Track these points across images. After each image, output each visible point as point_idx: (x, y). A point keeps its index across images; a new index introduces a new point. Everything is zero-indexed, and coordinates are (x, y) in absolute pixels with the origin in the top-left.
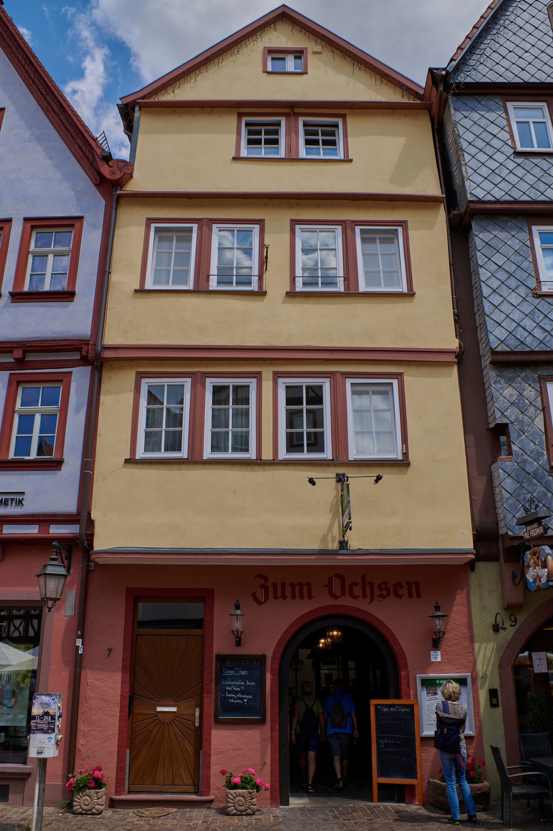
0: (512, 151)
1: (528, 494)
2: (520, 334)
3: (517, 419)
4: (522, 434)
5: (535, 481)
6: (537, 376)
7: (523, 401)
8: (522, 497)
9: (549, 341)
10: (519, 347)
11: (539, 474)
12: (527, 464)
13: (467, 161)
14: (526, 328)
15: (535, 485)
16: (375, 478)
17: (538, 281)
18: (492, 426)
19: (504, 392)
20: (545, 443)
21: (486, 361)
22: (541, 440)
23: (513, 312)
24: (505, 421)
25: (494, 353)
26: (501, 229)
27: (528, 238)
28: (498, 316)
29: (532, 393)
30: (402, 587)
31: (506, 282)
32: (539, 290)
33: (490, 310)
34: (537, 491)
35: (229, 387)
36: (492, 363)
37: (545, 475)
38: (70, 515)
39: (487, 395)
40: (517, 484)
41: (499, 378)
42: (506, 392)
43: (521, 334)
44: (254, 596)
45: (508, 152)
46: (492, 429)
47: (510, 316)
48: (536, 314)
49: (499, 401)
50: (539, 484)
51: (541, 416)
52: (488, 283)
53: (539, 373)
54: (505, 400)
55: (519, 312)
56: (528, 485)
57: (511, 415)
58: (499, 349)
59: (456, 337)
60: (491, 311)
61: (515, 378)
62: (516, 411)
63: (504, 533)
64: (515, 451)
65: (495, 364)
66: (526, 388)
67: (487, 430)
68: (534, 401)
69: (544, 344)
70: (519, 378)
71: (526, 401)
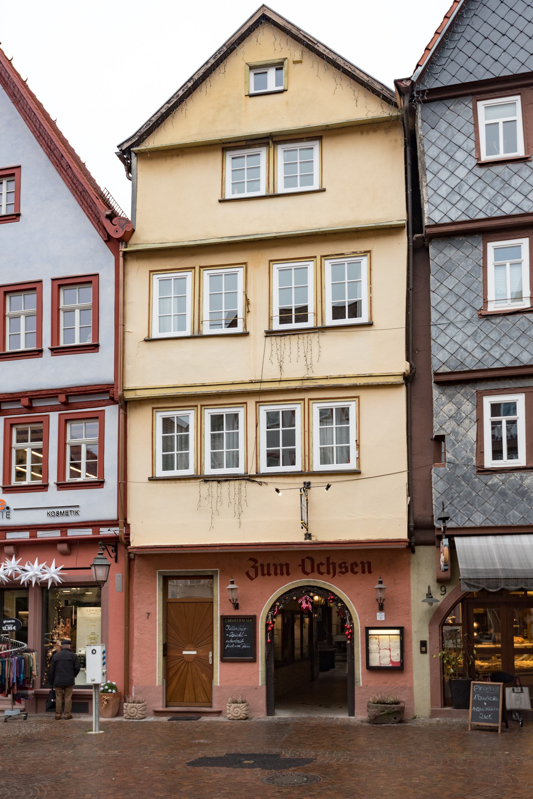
0: (474, 162)
1: (456, 493)
4: (456, 443)
5: (463, 483)
6: (475, 391)
7: (461, 414)
8: (450, 496)
10: (458, 367)
11: (467, 477)
12: (457, 469)
13: (428, 181)
14: (467, 349)
15: (463, 486)
16: (326, 487)
17: (485, 301)
19: (444, 408)
20: (475, 451)
22: (472, 447)
23: (457, 334)
24: (442, 433)
25: (436, 374)
26: (456, 250)
27: (482, 256)
28: (442, 340)
29: (468, 407)
31: (454, 305)
32: (485, 310)
33: (436, 335)
34: (464, 491)
35: (223, 415)
37: (471, 477)
38: (113, 521)
40: (447, 486)
43: (462, 355)
44: (247, 574)
45: (471, 164)
46: (434, 439)
47: (454, 339)
48: (479, 335)
49: (439, 416)
50: (466, 485)
52: (438, 308)
55: (462, 334)
56: (457, 486)
57: (448, 428)
58: (440, 371)
59: (408, 359)
60: (437, 336)
61: (456, 394)
62: (453, 423)
64: (449, 459)
65: (438, 383)
66: (464, 403)
67: (432, 439)
68: (470, 414)
69: (482, 363)
70: (459, 395)
71: (463, 415)
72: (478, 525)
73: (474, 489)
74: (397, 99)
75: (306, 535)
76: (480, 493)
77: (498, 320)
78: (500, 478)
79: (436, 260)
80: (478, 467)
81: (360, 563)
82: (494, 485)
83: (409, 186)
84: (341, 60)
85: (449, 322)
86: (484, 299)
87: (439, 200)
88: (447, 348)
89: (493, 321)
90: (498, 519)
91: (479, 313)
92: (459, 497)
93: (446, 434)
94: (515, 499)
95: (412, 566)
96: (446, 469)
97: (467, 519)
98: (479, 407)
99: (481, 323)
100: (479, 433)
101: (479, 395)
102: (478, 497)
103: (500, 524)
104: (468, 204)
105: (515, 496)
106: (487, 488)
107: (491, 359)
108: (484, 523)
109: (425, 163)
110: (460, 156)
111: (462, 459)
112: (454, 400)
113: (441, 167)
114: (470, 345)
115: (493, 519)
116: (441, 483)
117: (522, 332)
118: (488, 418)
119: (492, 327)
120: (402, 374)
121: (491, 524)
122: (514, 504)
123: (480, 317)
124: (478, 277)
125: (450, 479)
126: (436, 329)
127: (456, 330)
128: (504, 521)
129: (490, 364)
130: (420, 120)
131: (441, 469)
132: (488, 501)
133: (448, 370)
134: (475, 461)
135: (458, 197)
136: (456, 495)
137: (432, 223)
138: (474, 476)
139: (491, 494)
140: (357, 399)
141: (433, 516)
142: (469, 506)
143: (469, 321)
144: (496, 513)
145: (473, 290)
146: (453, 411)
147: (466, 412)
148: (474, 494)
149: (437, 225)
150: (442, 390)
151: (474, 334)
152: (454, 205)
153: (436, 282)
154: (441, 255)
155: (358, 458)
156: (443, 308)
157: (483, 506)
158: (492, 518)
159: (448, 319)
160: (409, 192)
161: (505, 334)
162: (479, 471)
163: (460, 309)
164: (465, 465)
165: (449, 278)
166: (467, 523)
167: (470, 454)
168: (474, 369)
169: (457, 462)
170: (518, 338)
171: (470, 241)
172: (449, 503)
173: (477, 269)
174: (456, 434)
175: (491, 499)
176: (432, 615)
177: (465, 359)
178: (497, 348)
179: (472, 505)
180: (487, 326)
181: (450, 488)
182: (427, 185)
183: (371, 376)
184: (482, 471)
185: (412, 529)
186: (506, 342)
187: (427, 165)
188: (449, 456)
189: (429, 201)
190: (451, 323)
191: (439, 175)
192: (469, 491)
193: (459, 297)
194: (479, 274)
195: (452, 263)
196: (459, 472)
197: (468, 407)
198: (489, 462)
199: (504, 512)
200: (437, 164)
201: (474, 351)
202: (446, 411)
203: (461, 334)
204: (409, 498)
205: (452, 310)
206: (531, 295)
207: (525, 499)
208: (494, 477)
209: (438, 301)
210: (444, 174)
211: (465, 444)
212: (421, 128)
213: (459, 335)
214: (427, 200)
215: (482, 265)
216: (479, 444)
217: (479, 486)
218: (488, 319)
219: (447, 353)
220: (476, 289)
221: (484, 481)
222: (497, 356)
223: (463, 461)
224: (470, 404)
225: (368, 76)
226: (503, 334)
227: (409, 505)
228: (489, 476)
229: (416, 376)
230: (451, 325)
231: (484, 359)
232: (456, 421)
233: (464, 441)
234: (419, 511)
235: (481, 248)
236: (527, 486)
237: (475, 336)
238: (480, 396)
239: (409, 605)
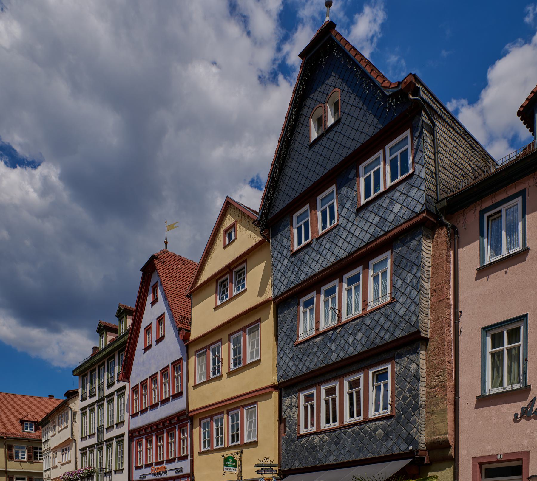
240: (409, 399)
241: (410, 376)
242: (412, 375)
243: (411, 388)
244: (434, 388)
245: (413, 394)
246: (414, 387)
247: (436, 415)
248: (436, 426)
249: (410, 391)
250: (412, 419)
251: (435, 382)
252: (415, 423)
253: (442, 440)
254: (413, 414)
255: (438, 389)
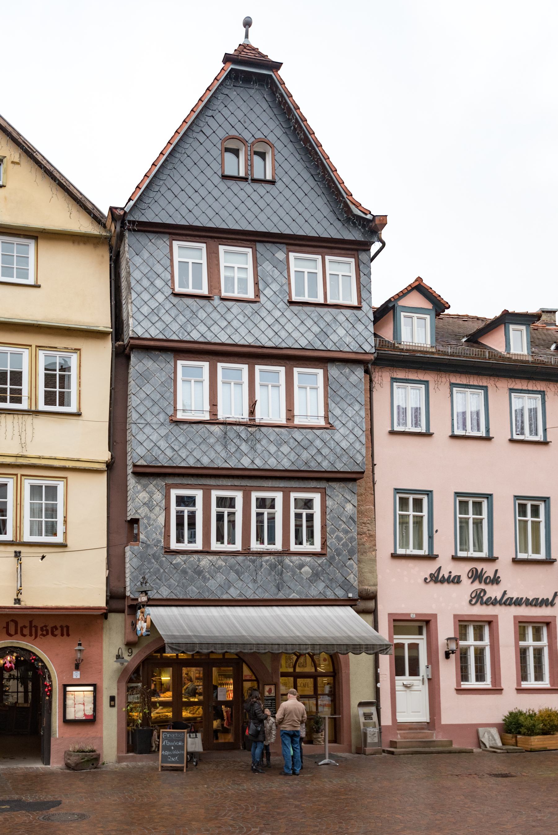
1: (147, 569)
2: (156, 451)
3: (146, 516)
4: (148, 526)
5: (153, 561)
6: (164, 484)
7: (152, 502)
8: (143, 571)
9: (176, 458)
12: (149, 548)
15: (153, 563)
18: (129, 519)
19: (140, 495)
21: (130, 470)
24: (137, 516)
25: (135, 466)
29: (159, 497)
30: (57, 629)
36: (134, 473)
37: (160, 557)
39: (128, 495)
41: (137, 484)
42: (140, 495)
46: (129, 521)
47: (150, 437)
50: (155, 563)
51: (164, 514)
53: (166, 482)
54: (139, 501)
56: (148, 563)
57: (142, 513)
58: (139, 463)
59: (109, 450)
61: (149, 485)
62: (146, 509)
63: (129, 595)
64: (142, 539)
65: (135, 473)
67: (126, 521)
68: (160, 503)
71: (155, 502)
72: (165, 597)
73: (161, 566)
74: (109, 222)
75: (15, 600)
76: (166, 571)
77: (185, 427)
78: (182, 558)
79: (136, 368)
80: (166, 548)
81: (60, 627)
82: (178, 564)
83: (113, 298)
84: (58, 173)
85: (146, 422)
86: (174, 408)
87: (142, 318)
88: (144, 444)
89: (181, 426)
90: (180, 593)
91: (171, 419)
92: (150, 573)
93: (140, 517)
94: (193, 576)
95: (105, 630)
96: (138, 548)
97: (156, 591)
98: (167, 498)
99: (172, 427)
100: (167, 520)
101: (167, 487)
102: (165, 574)
103: (181, 597)
104: (165, 326)
105: (194, 574)
106: (172, 566)
107: (179, 458)
108: (170, 595)
109: (130, 282)
110: (159, 283)
111: (153, 541)
112: (147, 489)
113: (143, 289)
114: (163, 444)
115: (176, 593)
116: (135, 560)
117: (203, 439)
118: (174, 508)
119: (180, 431)
120: (106, 462)
121: (175, 597)
122: (192, 580)
123: (171, 422)
124: (169, 388)
125: (143, 557)
126: (136, 427)
127: (152, 431)
128: (184, 595)
129: (178, 462)
130: (127, 245)
131: (136, 547)
132: (173, 577)
133: (145, 464)
134: (163, 543)
135: (157, 318)
136: (148, 571)
137: (135, 336)
138: (162, 555)
139: (175, 571)
140: (65, 480)
141: (125, 588)
142: (158, 581)
143: (162, 424)
144: (178, 588)
145: (166, 398)
146: (147, 499)
147: (157, 501)
148: (162, 571)
149: (139, 338)
150: (138, 480)
151: (166, 436)
152: (153, 324)
153: (137, 386)
154: (141, 364)
155: (65, 533)
156: (142, 409)
157: (169, 581)
158: (176, 591)
159: (145, 420)
160: (113, 303)
161: (190, 439)
162: (166, 552)
163: (155, 413)
164: (155, 546)
165: (147, 385)
166: (156, 595)
167: (159, 537)
168: (166, 465)
169: (148, 543)
170: (200, 444)
171: (164, 356)
172: (141, 577)
173: (169, 381)
174: (149, 518)
175: (175, 576)
176: (120, 674)
177: (159, 456)
178: (184, 450)
179: (160, 580)
180: (176, 430)
181: (143, 565)
182: (132, 302)
183: (79, 461)
184: (169, 552)
185: (108, 598)
186: (191, 446)
187: (132, 285)
188: (142, 537)
189: (134, 316)
190: (148, 424)
191: (142, 296)
192: (157, 568)
193: (155, 403)
194: (171, 386)
195: (150, 373)
196: (151, 552)
197: (158, 496)
198: (174, 545)
199: (184, 587)
200: (141, 286)
201: (166, 450)
202: (141, 498)
203: (156, 434)
204: (108, 571)
205: (148, 413)
206: (210, 409)
207: (201, 577)
208: (178, 558)
209: (138, 403)
210: (146, 296)
211: (155, 528)
212: (128, 252)
213: (154, 434)
214: (132, 315)
215: (173, 378)
216: (167, 529)
217: (166, 564)
218: (177, 425)
219: (144, 449)
220: (168, 398)
221: (170, 560)
222: (184, 456)
223: (154, 542)
224: (160, 494)
225: (81, 194)
226: (189, 438)
227: (107, 577)
228: (174, 557)
229: (114, 465)
230: (148, 425)
231: (174, 457)
232: (148, 507)
233: (155, 525)
234: (115, 584)
235: (173, 364)
236: (203, 567)
237: (166, 437)
238: (168, 488)
239: (101, 665)
240: (344, 540)
241: (345, 516)
242: (348, 515)
243: (347, 529)
244: (361, 535)
245: (349, 536)
246: (351, 528)
247: (364, 564)
248: (364, 576)
249: (346, 532)
250: (348, 563)
251: (362, 529)
252: (353, 568)
253: (371, 592)
254: (350, 557)
255: (365, 537)
